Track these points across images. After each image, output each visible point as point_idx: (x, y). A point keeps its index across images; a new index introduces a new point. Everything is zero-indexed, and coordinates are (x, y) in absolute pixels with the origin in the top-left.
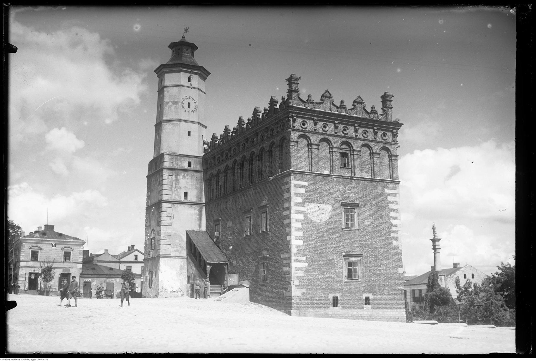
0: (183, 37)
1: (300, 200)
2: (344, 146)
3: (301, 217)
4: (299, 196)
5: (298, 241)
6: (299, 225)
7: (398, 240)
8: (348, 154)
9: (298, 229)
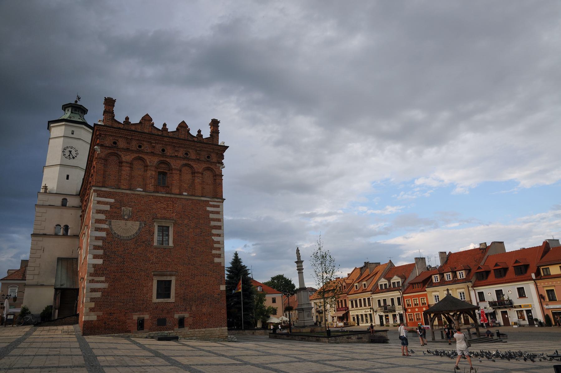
0: (76, 102)
1: (102, 217)
2: (163, 166)
3: (103, 234)
4: (102, 213)
5: (97, 259)
6: (100, 243)
7: (220, 257)
8: (167, 173)
9: (96, 248)
